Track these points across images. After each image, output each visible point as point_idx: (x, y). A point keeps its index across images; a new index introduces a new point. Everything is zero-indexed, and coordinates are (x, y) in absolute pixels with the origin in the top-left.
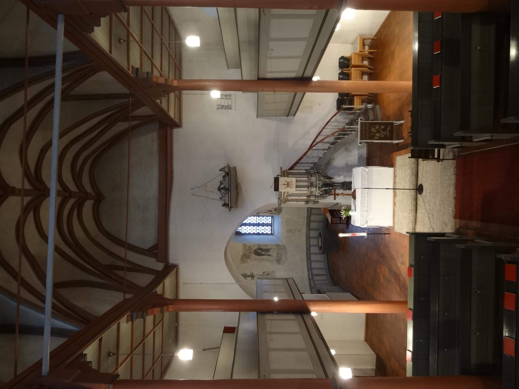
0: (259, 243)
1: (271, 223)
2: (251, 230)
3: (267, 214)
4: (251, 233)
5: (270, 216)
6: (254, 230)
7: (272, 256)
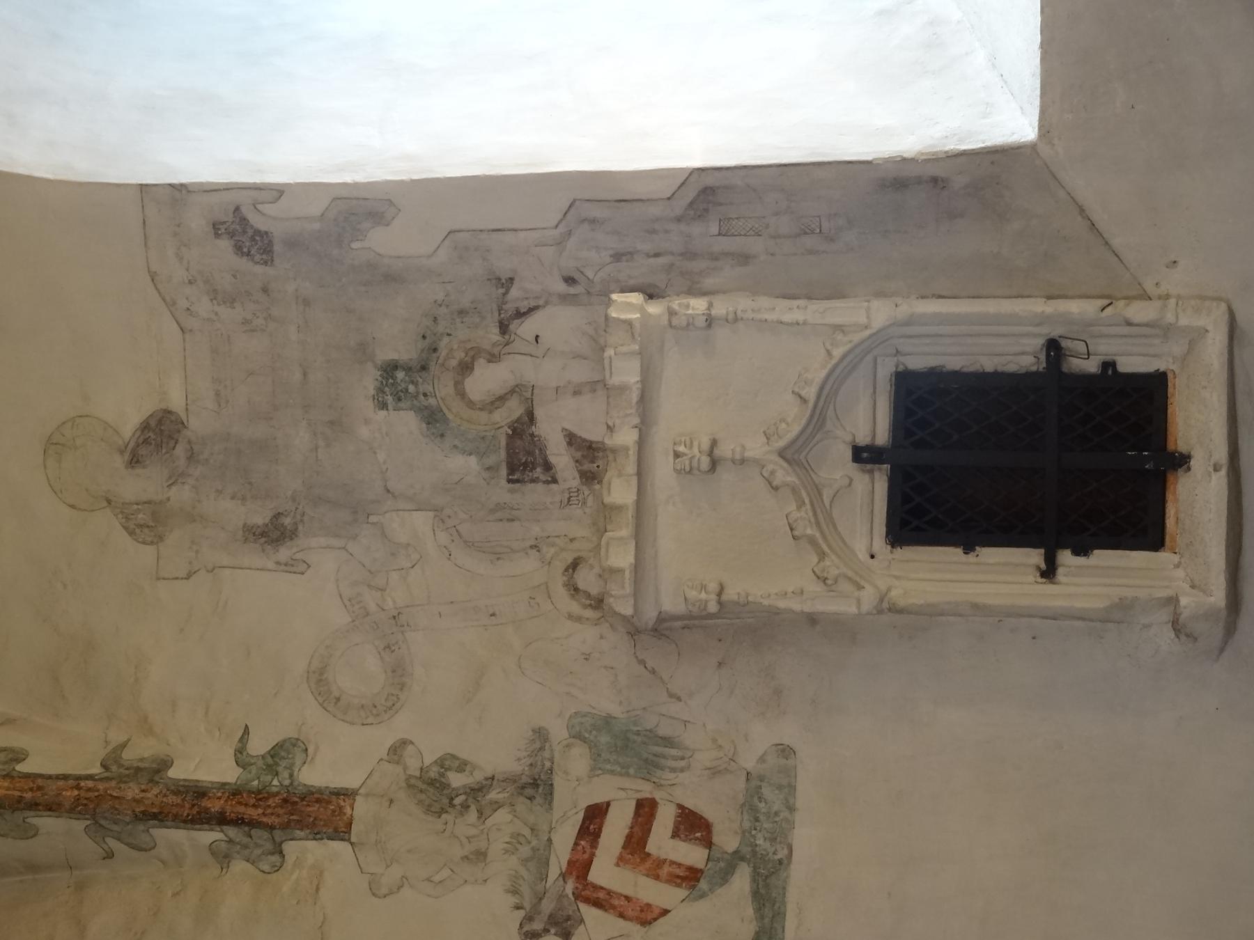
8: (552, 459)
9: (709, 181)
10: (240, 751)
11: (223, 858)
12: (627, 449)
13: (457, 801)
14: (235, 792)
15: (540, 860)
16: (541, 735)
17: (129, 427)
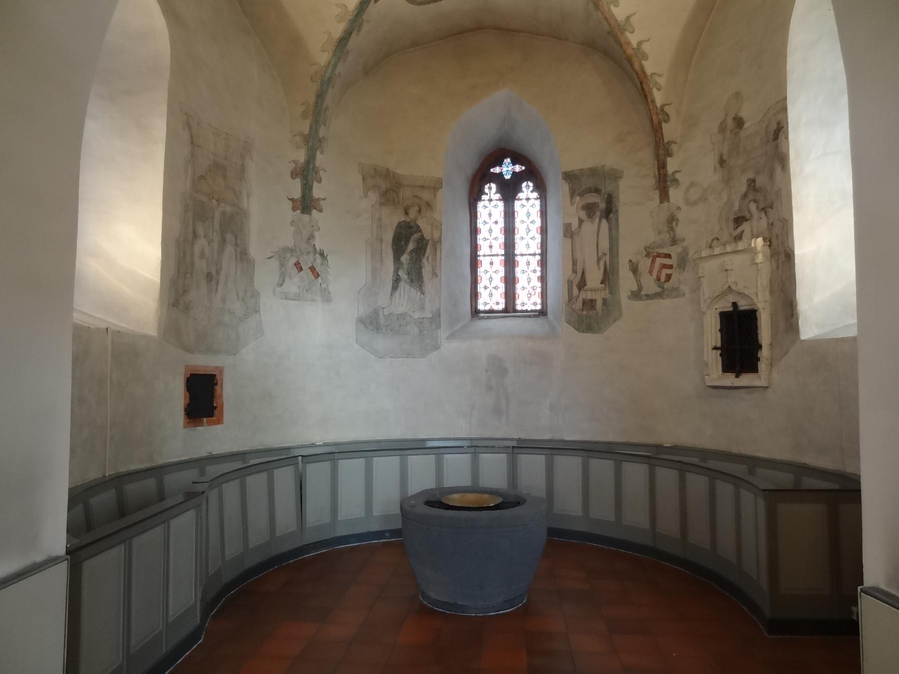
0: (445, 246)
1: (519, 308)
2: (487, 236)
4: (480, 237)
6: (491, 247)
7: (392, 295)
8: (738, 228)
9: (792, 256)
10: (676, 172)
11: (655, 177)
12: (725, 250)
13: (670, 225)
14: (665, 175)
15: (661, 246)
16: (684, 240)
17: (743, 114)
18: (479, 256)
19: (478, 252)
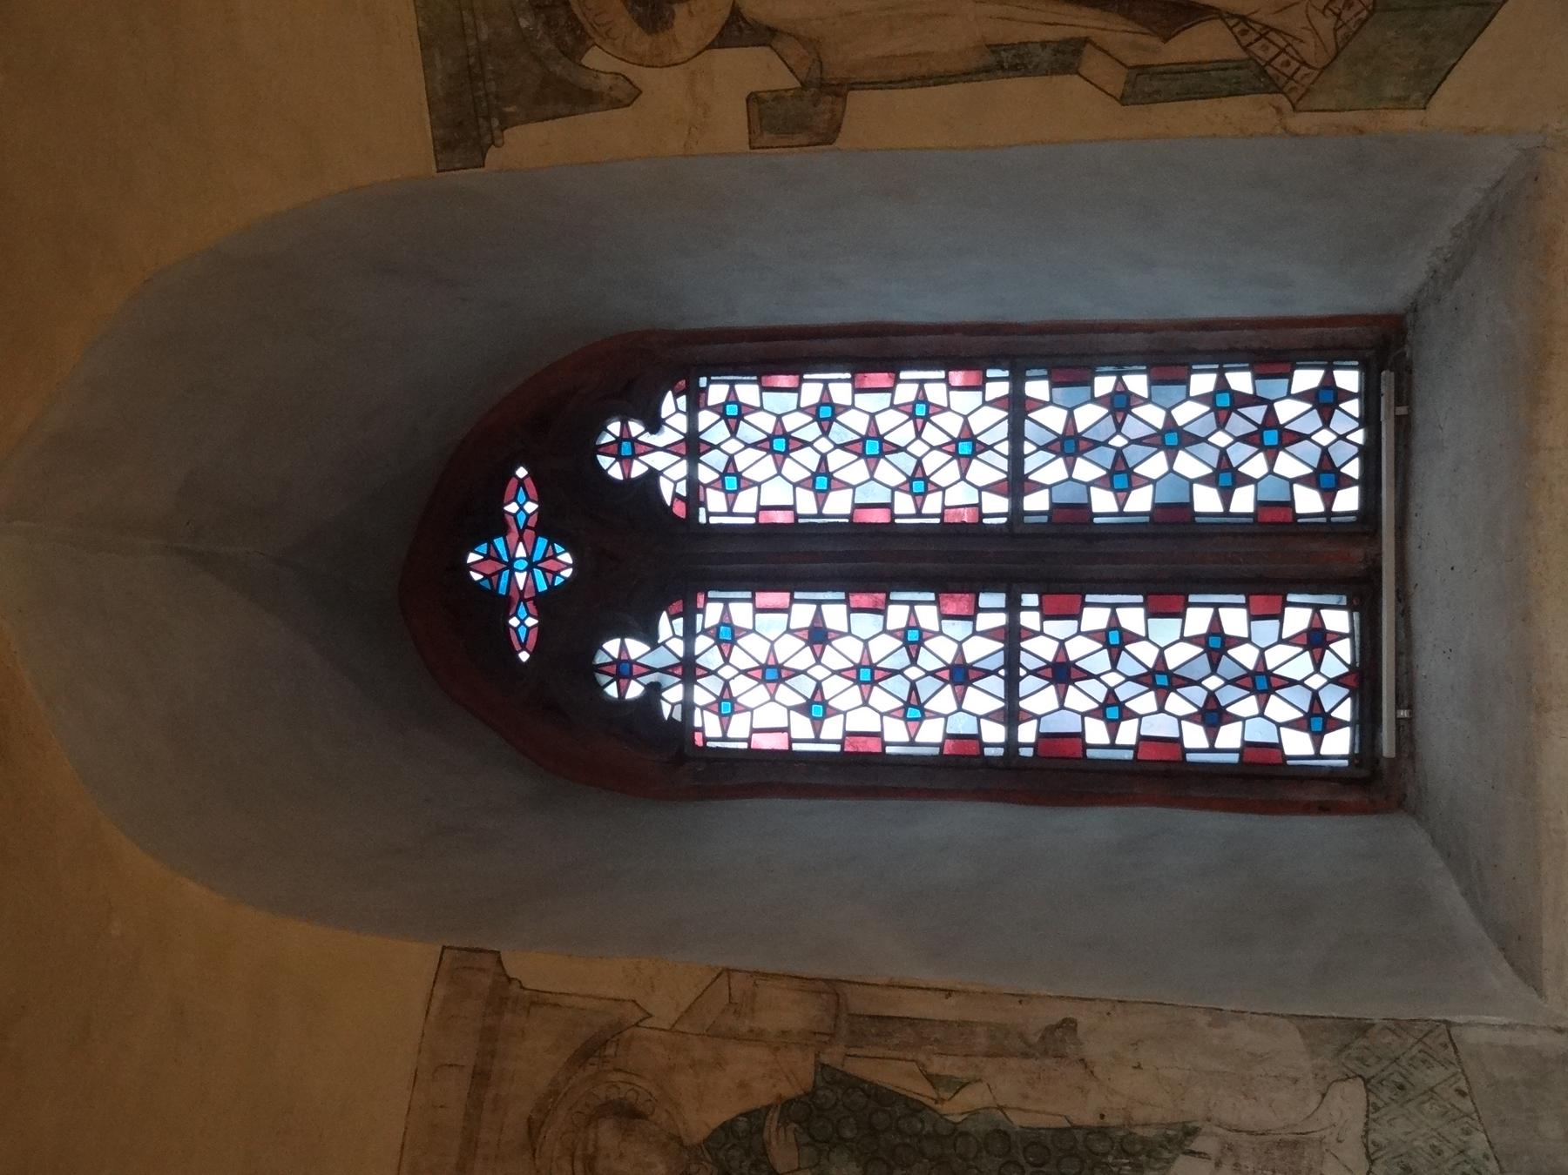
3: (1071, 84)
5: (1328, 357)
18: (1011, 744)
19: (988, 752)
